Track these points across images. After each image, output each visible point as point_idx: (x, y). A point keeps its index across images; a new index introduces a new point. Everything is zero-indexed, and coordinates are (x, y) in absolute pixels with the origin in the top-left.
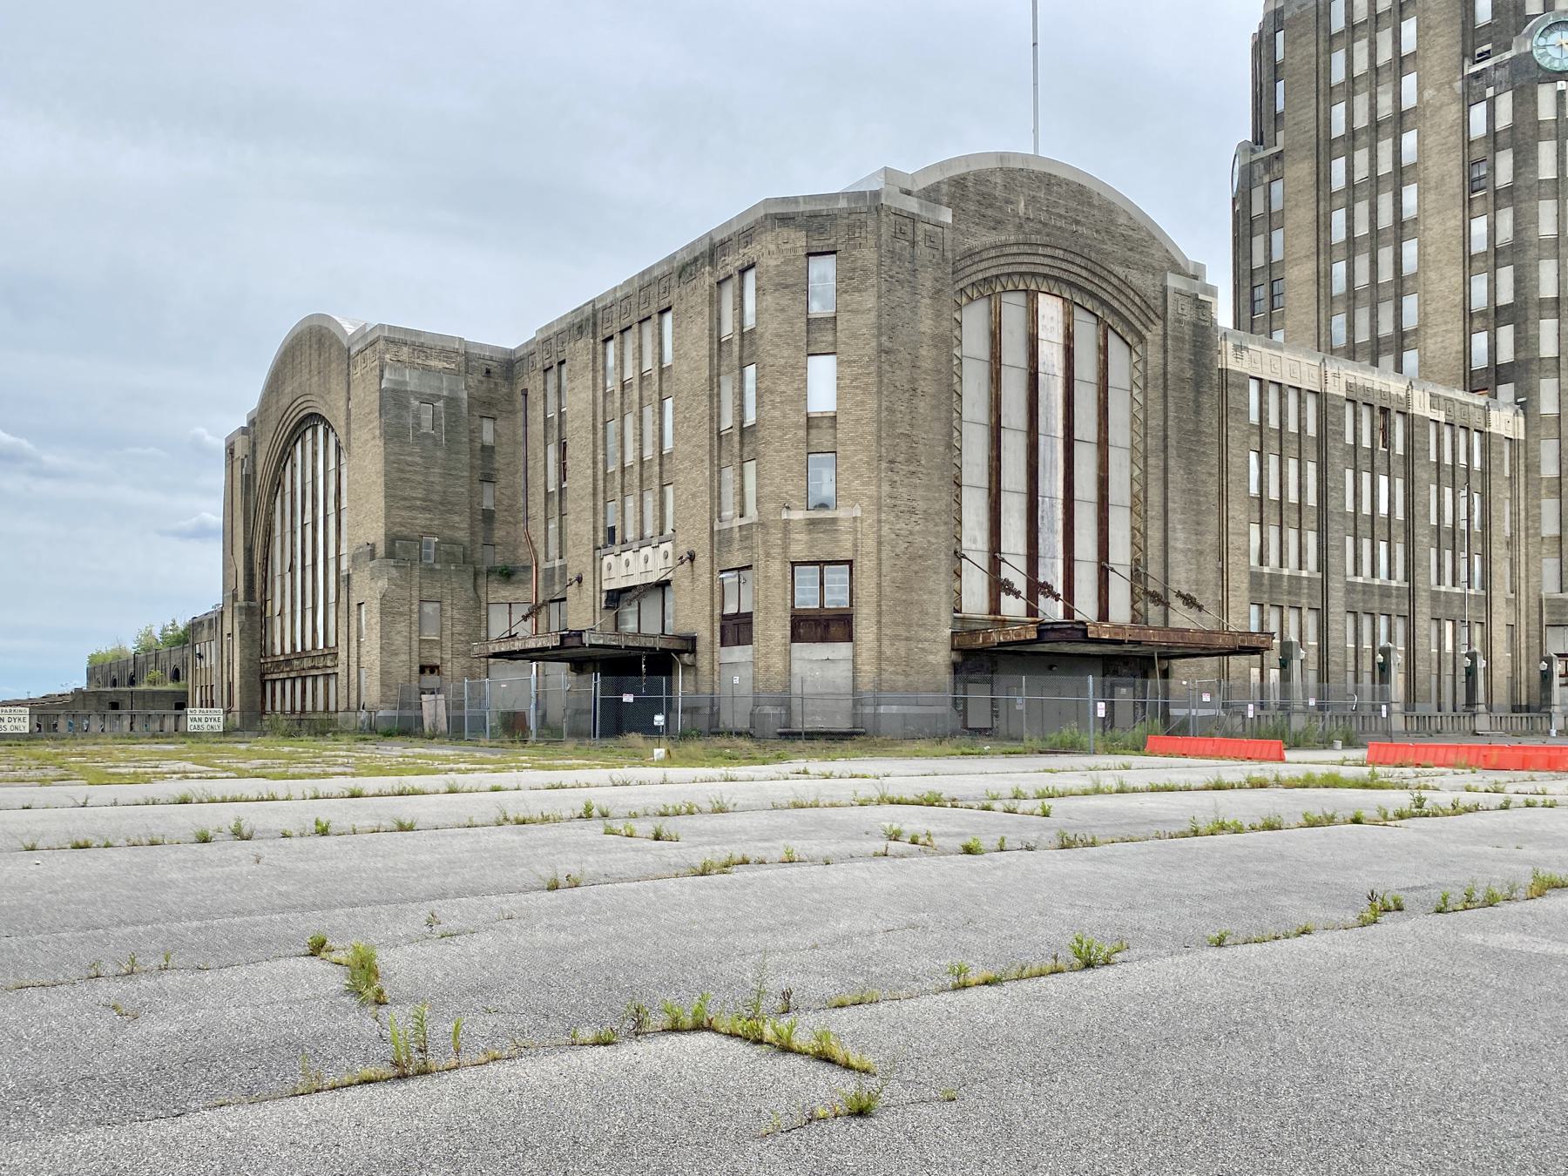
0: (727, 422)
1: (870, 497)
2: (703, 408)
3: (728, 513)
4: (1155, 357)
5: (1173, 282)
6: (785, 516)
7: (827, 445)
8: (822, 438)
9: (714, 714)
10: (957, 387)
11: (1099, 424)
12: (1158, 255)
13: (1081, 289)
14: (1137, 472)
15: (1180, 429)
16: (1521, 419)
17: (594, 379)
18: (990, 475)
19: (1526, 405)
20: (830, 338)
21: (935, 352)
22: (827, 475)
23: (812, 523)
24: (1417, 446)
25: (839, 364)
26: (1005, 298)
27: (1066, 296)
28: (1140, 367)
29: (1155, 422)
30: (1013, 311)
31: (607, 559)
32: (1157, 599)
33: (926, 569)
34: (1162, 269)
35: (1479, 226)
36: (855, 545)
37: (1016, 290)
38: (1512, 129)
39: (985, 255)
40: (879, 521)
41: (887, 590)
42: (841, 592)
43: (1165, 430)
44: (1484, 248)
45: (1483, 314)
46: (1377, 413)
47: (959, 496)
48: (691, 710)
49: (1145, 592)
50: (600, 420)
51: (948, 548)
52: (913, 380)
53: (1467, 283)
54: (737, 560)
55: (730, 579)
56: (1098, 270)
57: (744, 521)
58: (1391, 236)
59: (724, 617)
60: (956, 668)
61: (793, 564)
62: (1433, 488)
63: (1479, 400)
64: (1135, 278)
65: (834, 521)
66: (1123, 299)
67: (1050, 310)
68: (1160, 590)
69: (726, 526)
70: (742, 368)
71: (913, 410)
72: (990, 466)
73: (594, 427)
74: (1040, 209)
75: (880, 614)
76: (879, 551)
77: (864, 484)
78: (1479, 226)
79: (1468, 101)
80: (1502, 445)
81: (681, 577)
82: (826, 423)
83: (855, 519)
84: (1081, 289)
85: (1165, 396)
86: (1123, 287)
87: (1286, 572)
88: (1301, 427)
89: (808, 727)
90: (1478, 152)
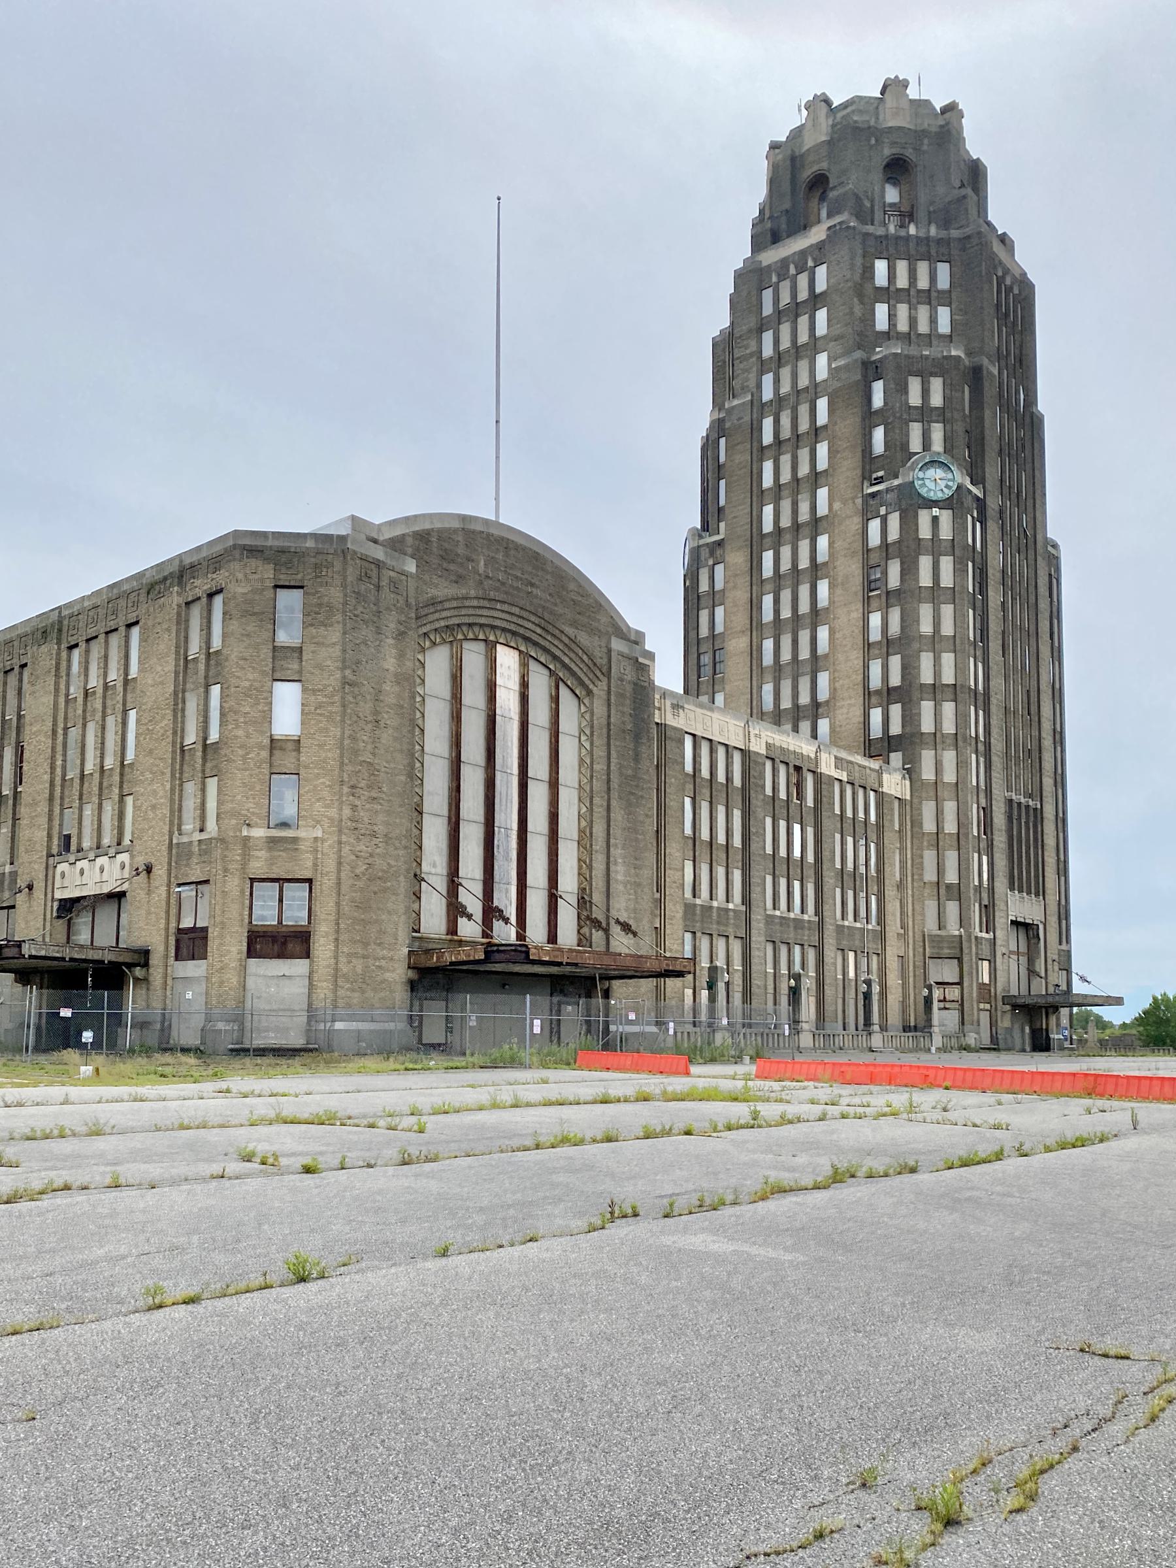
0: (191, 737)
1: (331, 819)
3: (187, 827)
4: (599, 708)
5: (617, 645)
6: (245, 833)
7: (291, 768)
8: (287, 761)
9: (166, 1030)
10: (420, 722)
11: (551, 765)
12: (604, 620)
13: (536, 644)
14: (584, 810)
15: (621, 774)
16: (908, 783)
18: (450, 804)
19: (911, 771)
20: (296, 666)
21: (397, 689)
22: (290, 795)
23: (272, 842)
24: (824, 799)
25: (304, 690)
26: (466, 645)
27: (523, 648)
28: (587, 716)
30: (473, 657)
32: (597, 924)
33: (385, 890)
34: (607, 633)
35: (875, 619)
36: (315, 865)
37: (476, 639)
38: (899, 542)
39: (447, 605)
40: (340, 843)
41: (346, 909)
42: (300, 908)
43: (608, 774)
44: (879, 638)
45: (878, 692)
46: (792, 770)
47: (420, 823)
48: (142, 1025)
49: (586, 919)
51: (408, 871)
52: (376, 712)
53: (866, 667)
54: (196, 874)
55: (188, 892)
56: (550, 628)
57: (204, 836)
58: (808, 621)
60: (413, 986)
61: (252, 880)
62: (838, 836)
63: (875, 764)
64: (583, 638)
65: (295, 840)
66: (572, 655)
68: (601, 917)
69: (185, 839)
70: (207, 687)
71: (375, 740)
72: (450, 797)
74: (498, 569)
75: (337, 931)
76: (339, 871)
77: (327, 806)
78: (875, 619)
80: (891, 803)
81: (136, 890)
82: (290, 746)
83: (316, 839)
84: (536, 644)
85: (609, 745)
86: (573, 646)
88: (729, 779)
89: (259, 1042)
90: (874, 558)
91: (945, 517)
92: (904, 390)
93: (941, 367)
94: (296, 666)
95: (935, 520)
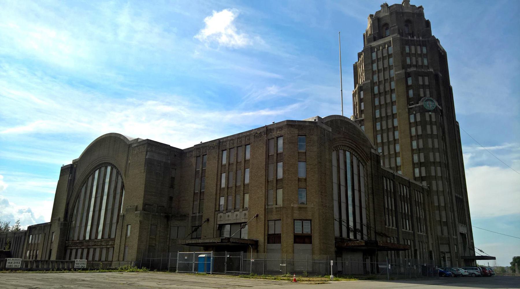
2: (263, 172)
4: (369, 169)
6: (292, 205)
8: (302, 184)
17: (218, 161)
22: (304, 194)
23: (300, 208)
29: (370, 186)
31: (219, 215)
45: (417, 164)
50: (219, 173)
54: (275, 217)
57: (277, 206)
59: (268, 235)
61: (294, 220)
67: (348, 154)
69: (270, 207)
73: (217, 175)
79: (409, 113)
84: (354, 150)
87: (390, 227)
91: (433, 115)
92: (417, 80)
93: (428, 74)
94: (304, 157)
95: (430, 116)
